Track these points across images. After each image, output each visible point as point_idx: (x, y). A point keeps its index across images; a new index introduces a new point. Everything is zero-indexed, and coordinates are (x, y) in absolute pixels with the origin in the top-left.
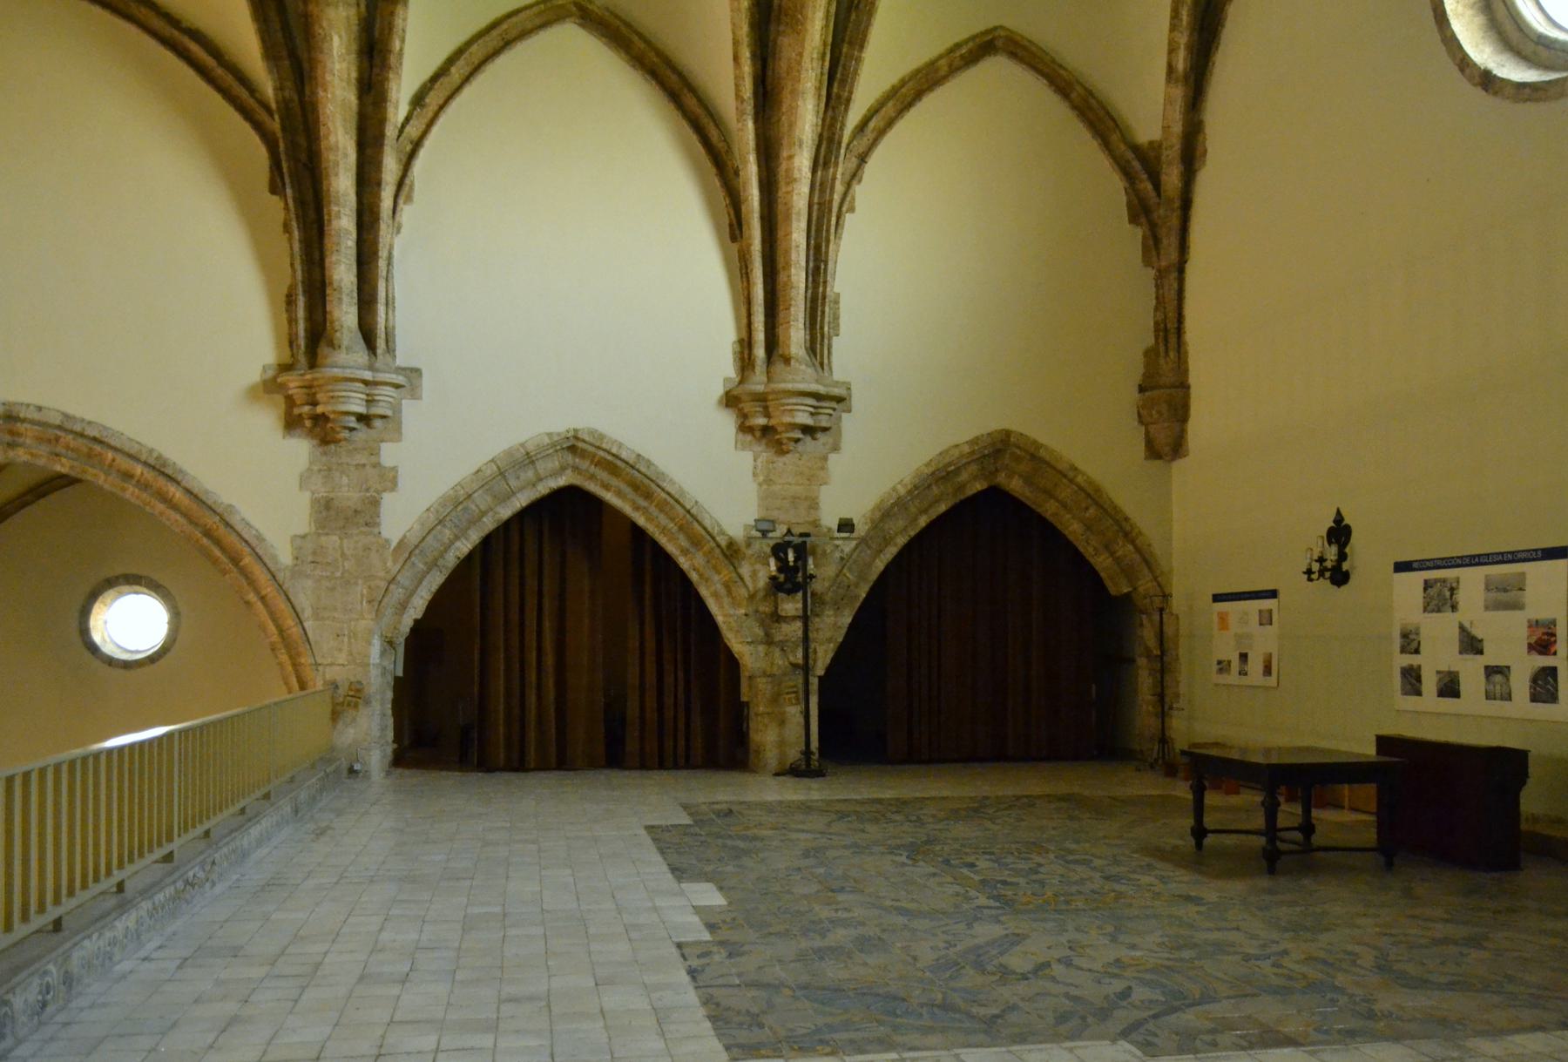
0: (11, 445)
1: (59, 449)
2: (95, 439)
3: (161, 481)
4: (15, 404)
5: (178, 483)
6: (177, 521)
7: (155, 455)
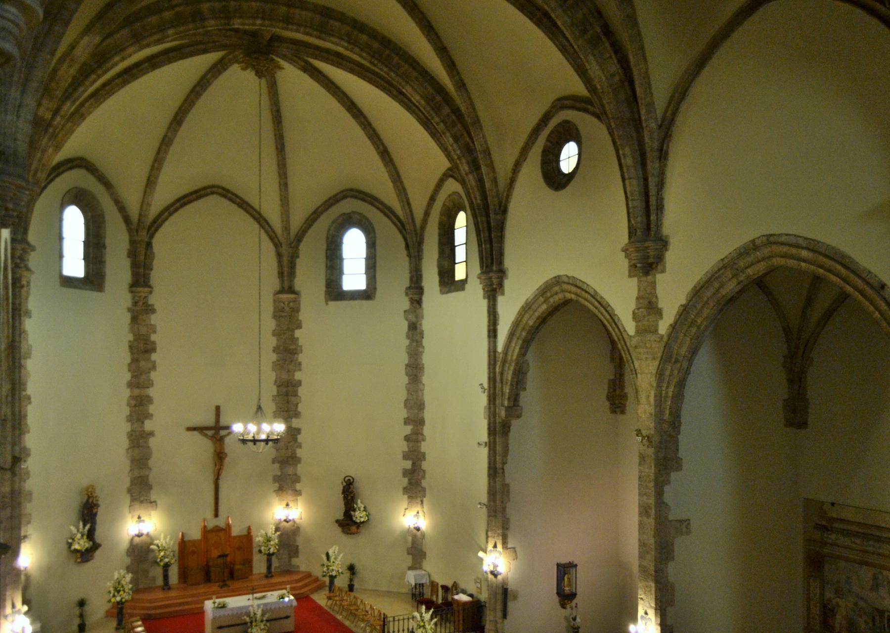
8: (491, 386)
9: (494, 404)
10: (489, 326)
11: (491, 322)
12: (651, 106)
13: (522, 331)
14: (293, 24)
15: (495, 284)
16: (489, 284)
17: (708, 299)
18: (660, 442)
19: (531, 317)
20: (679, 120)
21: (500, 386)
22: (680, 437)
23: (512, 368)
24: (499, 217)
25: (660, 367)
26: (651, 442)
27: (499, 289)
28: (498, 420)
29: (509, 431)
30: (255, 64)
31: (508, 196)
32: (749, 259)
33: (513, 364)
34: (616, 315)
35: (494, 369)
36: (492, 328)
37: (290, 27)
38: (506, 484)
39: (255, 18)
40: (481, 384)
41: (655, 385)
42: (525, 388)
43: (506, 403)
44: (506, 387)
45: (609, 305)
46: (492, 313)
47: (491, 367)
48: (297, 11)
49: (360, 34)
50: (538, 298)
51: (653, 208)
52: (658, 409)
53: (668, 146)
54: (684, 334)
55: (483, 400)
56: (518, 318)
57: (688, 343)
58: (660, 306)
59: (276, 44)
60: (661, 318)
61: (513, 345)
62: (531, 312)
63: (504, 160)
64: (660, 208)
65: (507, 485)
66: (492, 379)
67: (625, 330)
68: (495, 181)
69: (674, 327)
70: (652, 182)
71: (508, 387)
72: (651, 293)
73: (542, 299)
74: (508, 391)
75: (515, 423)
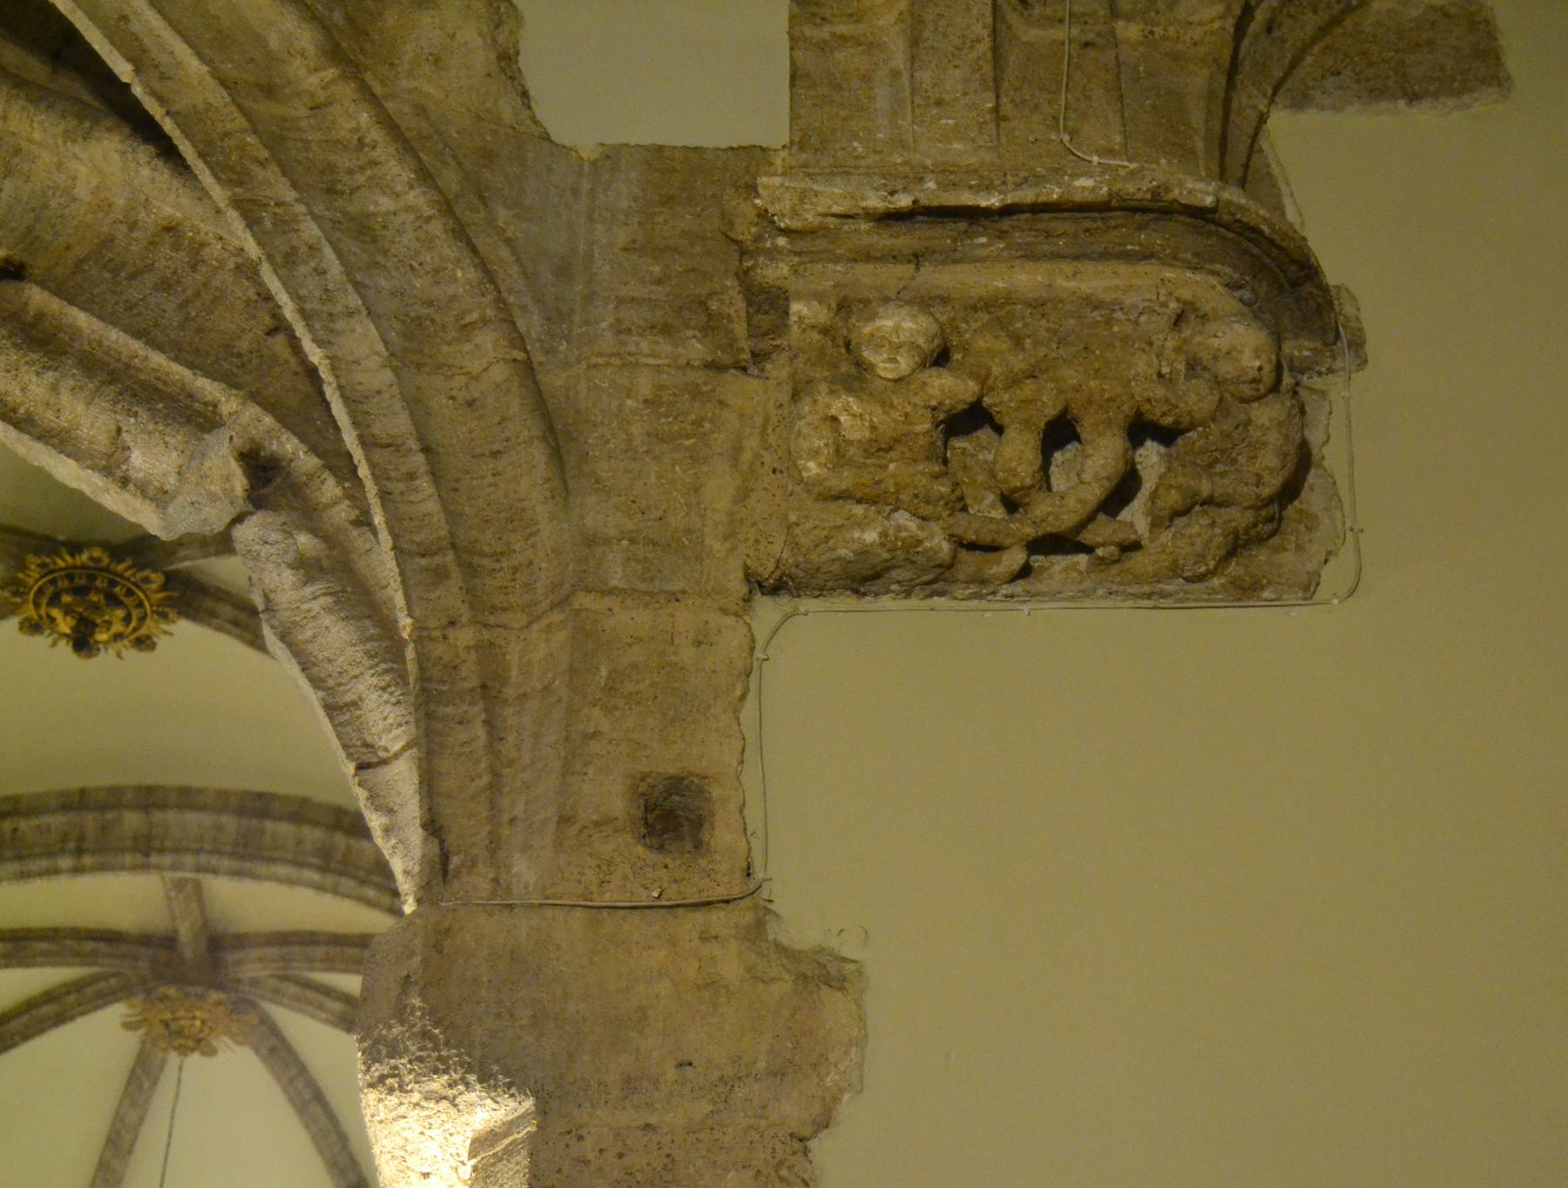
14: (162, 851)
30: (168, 1016)
37: (154, 859)
39: (50, 854)
48: (171, 816)
49: (352, 841)
59: (231, 957)
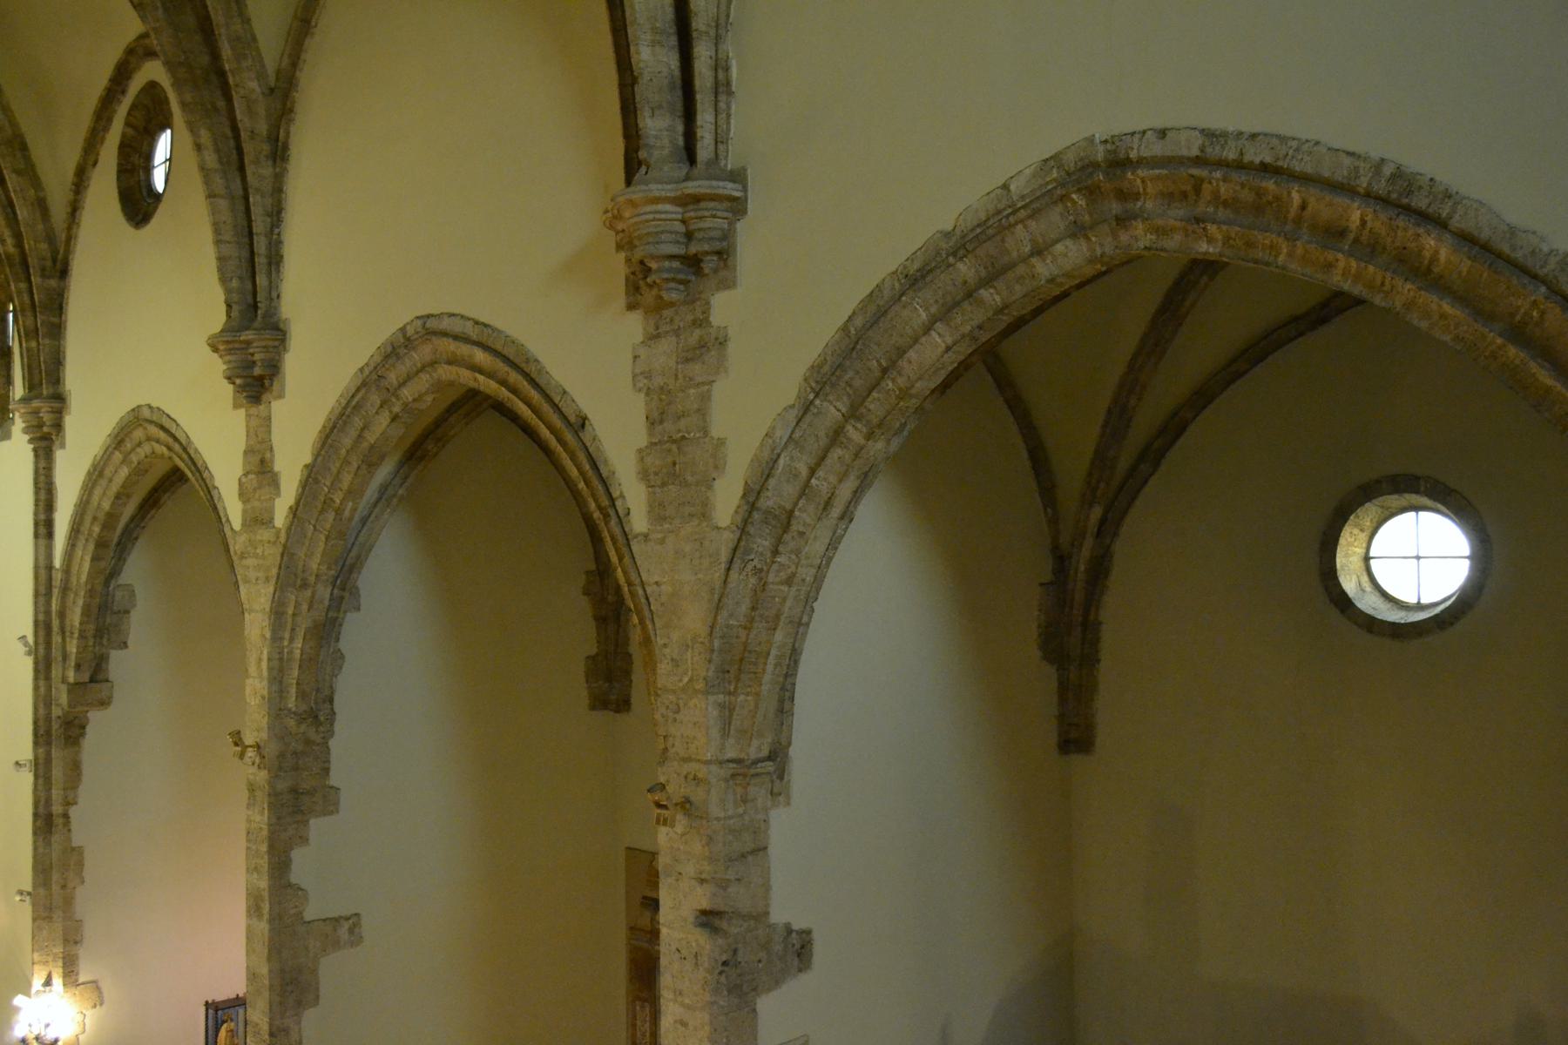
0: (1122, 221)
1: (1202, 208)
2: (1264, 168)
3: (1406, 231)
4: (1121, 137)
5: (1441, 224)
6: (1443, 316)
7: (1388, 170)
8: (41, 640)
9: (48, 678)
10: (36, 514)
11: (42, 504)
12: (245, 44)
13: (92, 524)
15: (48, 423)
16: (35, 423)
17: (348, 451)
18: (282, 755)
19: (104, 493)
20: (303, 77)
21: (60, 640)
22: (333, 743)
23: (80, 602)
24: (53, 283)
25: (276, 596)
26: (264, 757)
27: (57, 435)
28: (56, 712)
29: (83, 735)
31: (70, 239)
32: (403, 368)
33: (82, 593)
34: (216, 488)
35: (48, 603)
36: (42, 517)
38: (73, 849)
40: (24, 637)
41: (268, 635)
42: (125, 643)
43: (71, 676)
44: (70, 642)
45: (207, 468)
46: (41, 485)
47: (42, 600)
50: (112, 453)
51: (261, 261)
52: (275, 688)
53: (288, 133)
54: (314, 526)
55: (25, 667)
56: (83, 495)
57: (322, 545)
58: (277, 468)
60: (278, 494)
61: (79, 553)
62: (103, 482)
63: (56, 164)
64: (275, 260)
65: (79, 851)
66: (43, 626)
67: (228, 520)
68: (42, 206)
69: (294, 512)
70: (258, 205)
71: (75, 642)
72: (262, 442)
73: (118, 456)
74: (74, 650)
75: (95, 717)
